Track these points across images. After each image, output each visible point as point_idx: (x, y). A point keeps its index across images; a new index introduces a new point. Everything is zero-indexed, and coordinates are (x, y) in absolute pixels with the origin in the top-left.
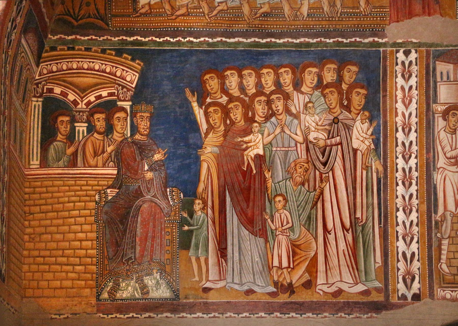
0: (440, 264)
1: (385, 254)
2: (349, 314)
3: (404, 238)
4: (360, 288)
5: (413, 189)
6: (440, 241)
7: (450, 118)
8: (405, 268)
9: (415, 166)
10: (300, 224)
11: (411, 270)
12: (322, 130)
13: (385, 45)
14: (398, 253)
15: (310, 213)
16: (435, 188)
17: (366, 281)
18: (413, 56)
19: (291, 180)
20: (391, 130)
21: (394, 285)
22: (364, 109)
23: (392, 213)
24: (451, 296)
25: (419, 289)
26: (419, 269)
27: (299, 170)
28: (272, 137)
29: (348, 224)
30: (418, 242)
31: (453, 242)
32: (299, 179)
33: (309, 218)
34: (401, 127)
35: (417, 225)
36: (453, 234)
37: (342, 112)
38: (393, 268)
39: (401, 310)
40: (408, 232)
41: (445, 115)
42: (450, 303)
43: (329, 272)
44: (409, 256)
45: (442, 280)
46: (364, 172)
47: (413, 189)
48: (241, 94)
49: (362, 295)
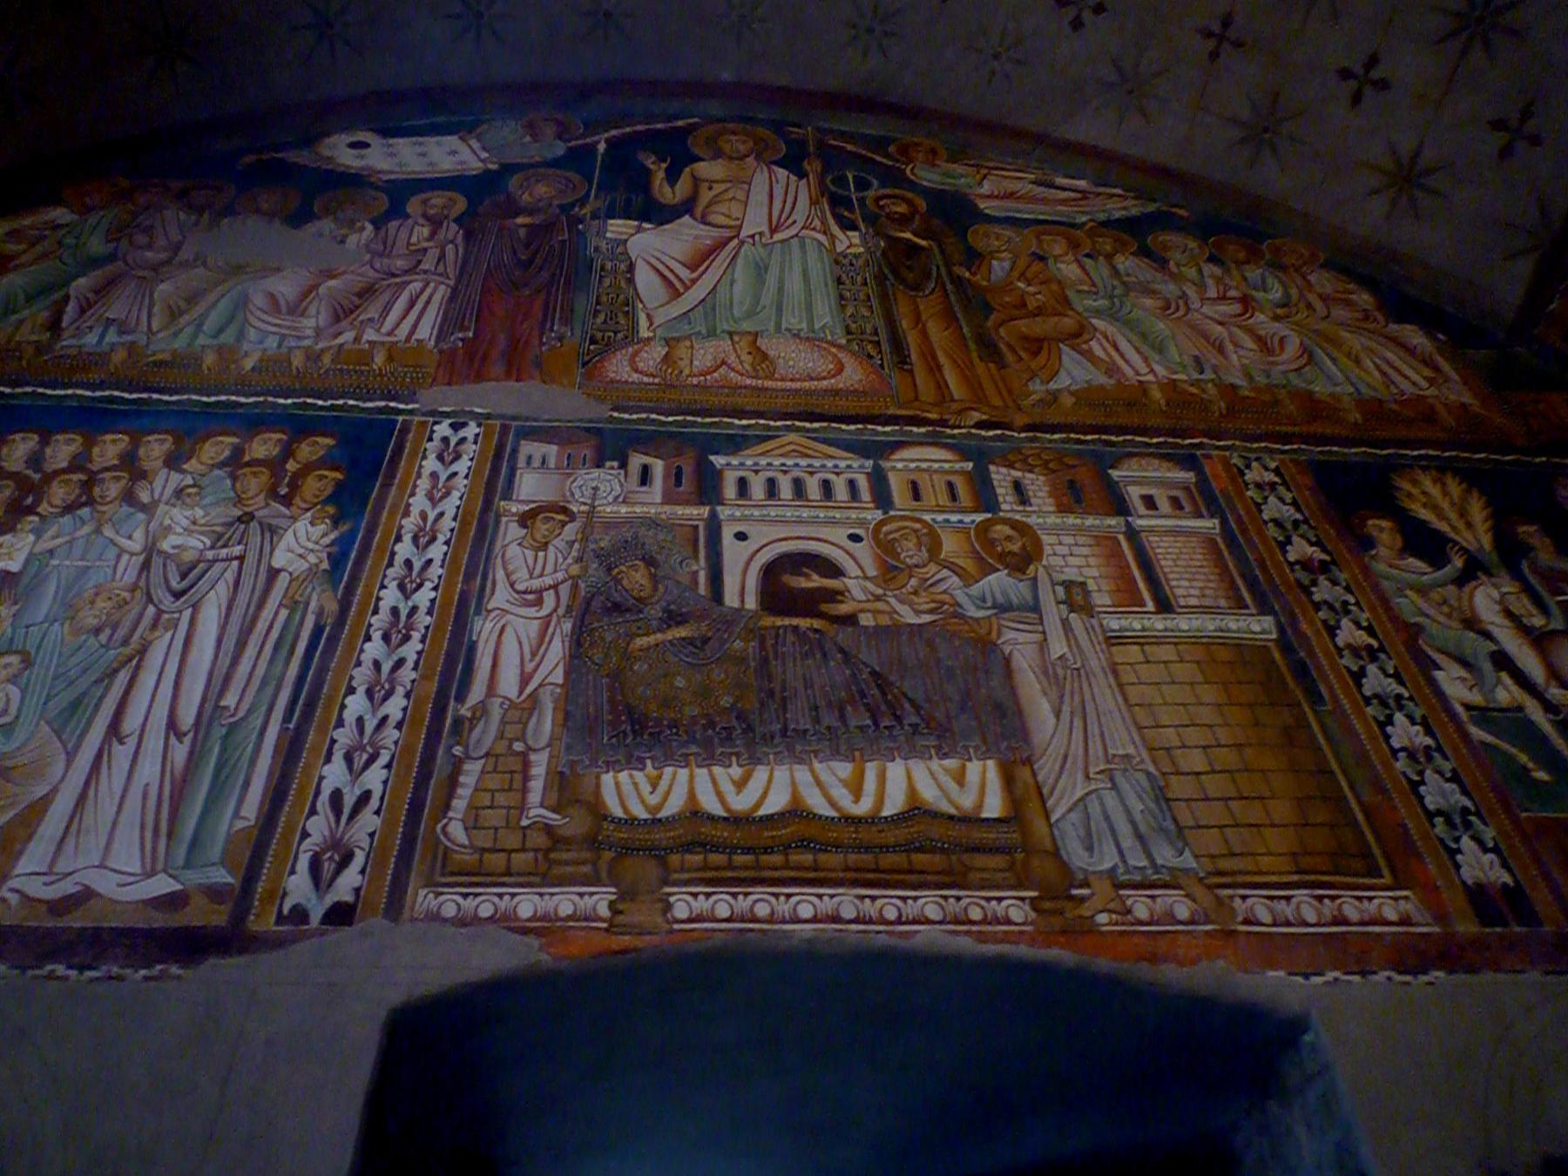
0: (445, 821)
1: (277, 796)
2: (82, 968)
3: (348, 758)
4: (163, 885)
5: (410, 650)
6: (457, 766)
7: (538, 523)
8: (327, 833)
9: (428, 604)
10: (41, 717)
11: (346, 837)
12: (202, 533)
13: (411, 412)
14: (317, 793)
15: (84, 694)
16: (472, 647)
17: (188, 865)
18: (471, 430)
19: (67, 625)
20: (385, 538)
21: (278, 877)
22: (327, 501)
23: (331, 698)
24: (459, 909)
25: (357, 890)
26: (372, 835)
27: (100, 604)
28: (60, 541)
29: (187, 718)
30: (388, 766)
31: (496, 766)
32: (92, 622)
33: (75, 705)
34: (410, 535)
35: (399, 726)
36: (501, 748)
37: (268, 505)
38: (290, 828)
39: (277, 956)
40: (365, 741)
41: (525, 520)
42: (450, 930)
43: (71, 840)
44: (349, 801)
45: (439, 865)
46: (284, 613)
47: (410, 650)
48: (27, 468)
49: (154, 908)
